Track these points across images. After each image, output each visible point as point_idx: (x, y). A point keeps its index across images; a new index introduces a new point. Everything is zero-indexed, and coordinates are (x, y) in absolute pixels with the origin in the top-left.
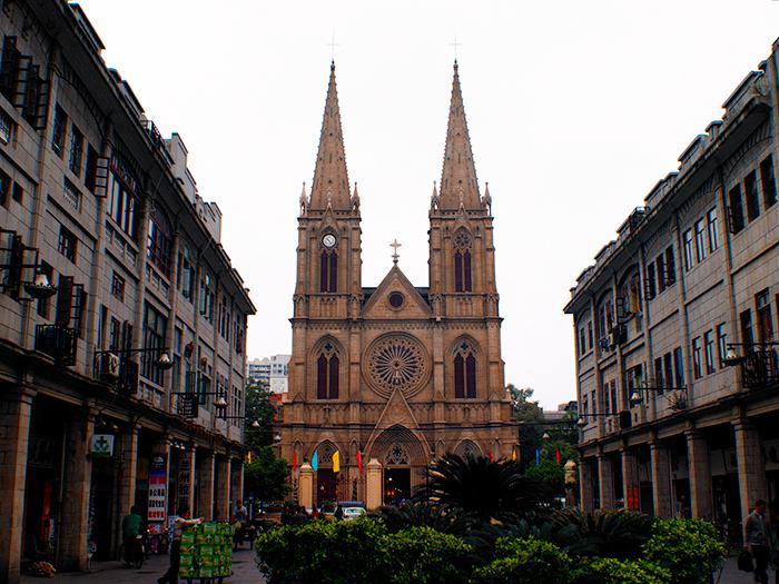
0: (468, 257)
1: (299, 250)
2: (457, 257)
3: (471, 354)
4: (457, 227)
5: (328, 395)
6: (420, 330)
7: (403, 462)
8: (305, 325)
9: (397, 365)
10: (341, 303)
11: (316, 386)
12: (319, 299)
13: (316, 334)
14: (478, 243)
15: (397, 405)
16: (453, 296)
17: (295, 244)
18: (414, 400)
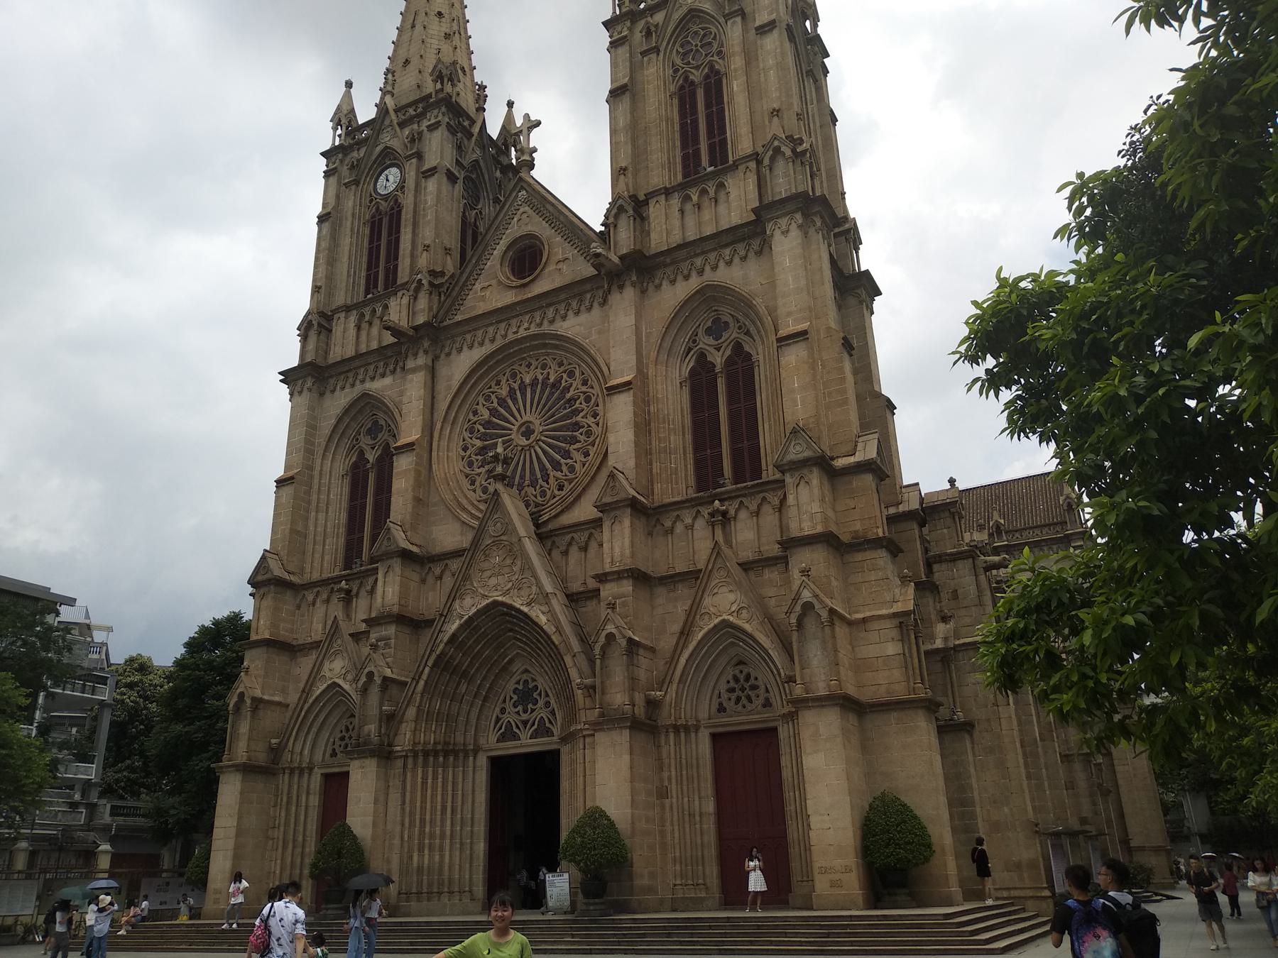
0: (715, 84)
1: (322, 219)
2: (685, 95)
3: (738, 347)
4: (677, 16)
5: (365, 556)
6: (583, 317)
7: (543, 730)
8: (309, 383)
9: (528, 433)
10: (397, 311)
11: (335, 544)
12: (353, 318)
13: (339, 401)
14: (734, 33)
15: (497, 543)
16: (667, 192)
17: (318, 209)
18: (566, 519)
